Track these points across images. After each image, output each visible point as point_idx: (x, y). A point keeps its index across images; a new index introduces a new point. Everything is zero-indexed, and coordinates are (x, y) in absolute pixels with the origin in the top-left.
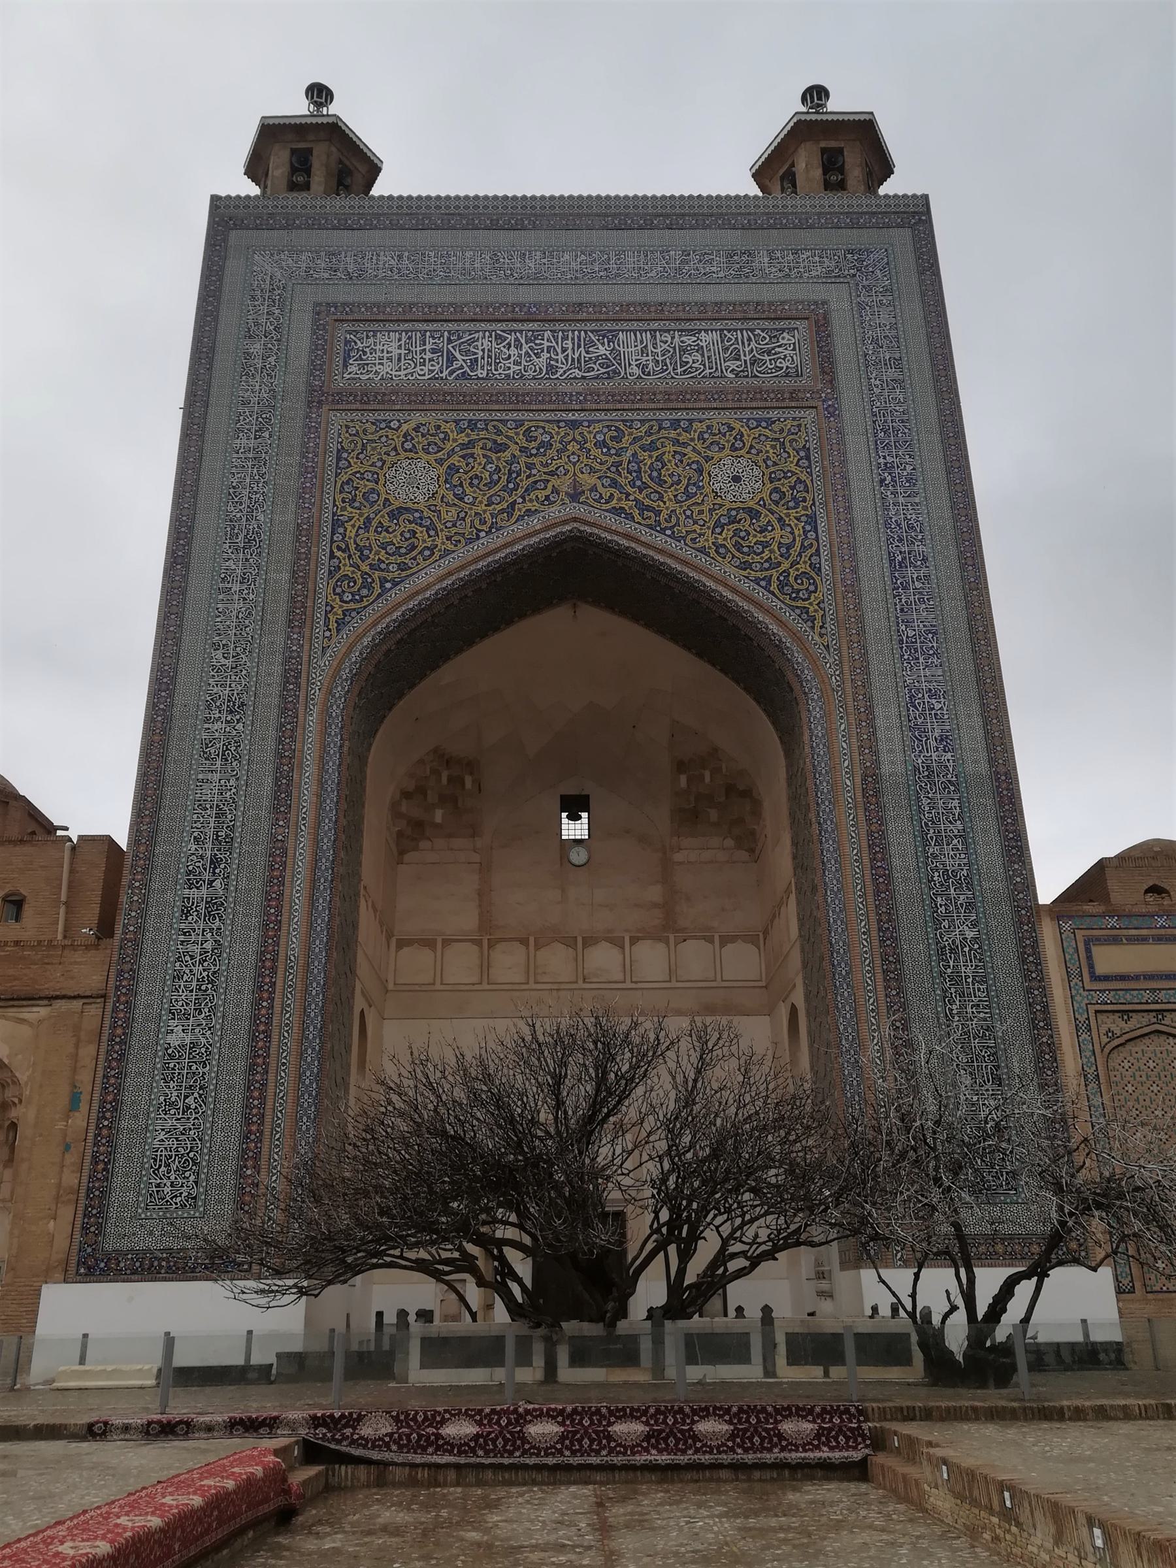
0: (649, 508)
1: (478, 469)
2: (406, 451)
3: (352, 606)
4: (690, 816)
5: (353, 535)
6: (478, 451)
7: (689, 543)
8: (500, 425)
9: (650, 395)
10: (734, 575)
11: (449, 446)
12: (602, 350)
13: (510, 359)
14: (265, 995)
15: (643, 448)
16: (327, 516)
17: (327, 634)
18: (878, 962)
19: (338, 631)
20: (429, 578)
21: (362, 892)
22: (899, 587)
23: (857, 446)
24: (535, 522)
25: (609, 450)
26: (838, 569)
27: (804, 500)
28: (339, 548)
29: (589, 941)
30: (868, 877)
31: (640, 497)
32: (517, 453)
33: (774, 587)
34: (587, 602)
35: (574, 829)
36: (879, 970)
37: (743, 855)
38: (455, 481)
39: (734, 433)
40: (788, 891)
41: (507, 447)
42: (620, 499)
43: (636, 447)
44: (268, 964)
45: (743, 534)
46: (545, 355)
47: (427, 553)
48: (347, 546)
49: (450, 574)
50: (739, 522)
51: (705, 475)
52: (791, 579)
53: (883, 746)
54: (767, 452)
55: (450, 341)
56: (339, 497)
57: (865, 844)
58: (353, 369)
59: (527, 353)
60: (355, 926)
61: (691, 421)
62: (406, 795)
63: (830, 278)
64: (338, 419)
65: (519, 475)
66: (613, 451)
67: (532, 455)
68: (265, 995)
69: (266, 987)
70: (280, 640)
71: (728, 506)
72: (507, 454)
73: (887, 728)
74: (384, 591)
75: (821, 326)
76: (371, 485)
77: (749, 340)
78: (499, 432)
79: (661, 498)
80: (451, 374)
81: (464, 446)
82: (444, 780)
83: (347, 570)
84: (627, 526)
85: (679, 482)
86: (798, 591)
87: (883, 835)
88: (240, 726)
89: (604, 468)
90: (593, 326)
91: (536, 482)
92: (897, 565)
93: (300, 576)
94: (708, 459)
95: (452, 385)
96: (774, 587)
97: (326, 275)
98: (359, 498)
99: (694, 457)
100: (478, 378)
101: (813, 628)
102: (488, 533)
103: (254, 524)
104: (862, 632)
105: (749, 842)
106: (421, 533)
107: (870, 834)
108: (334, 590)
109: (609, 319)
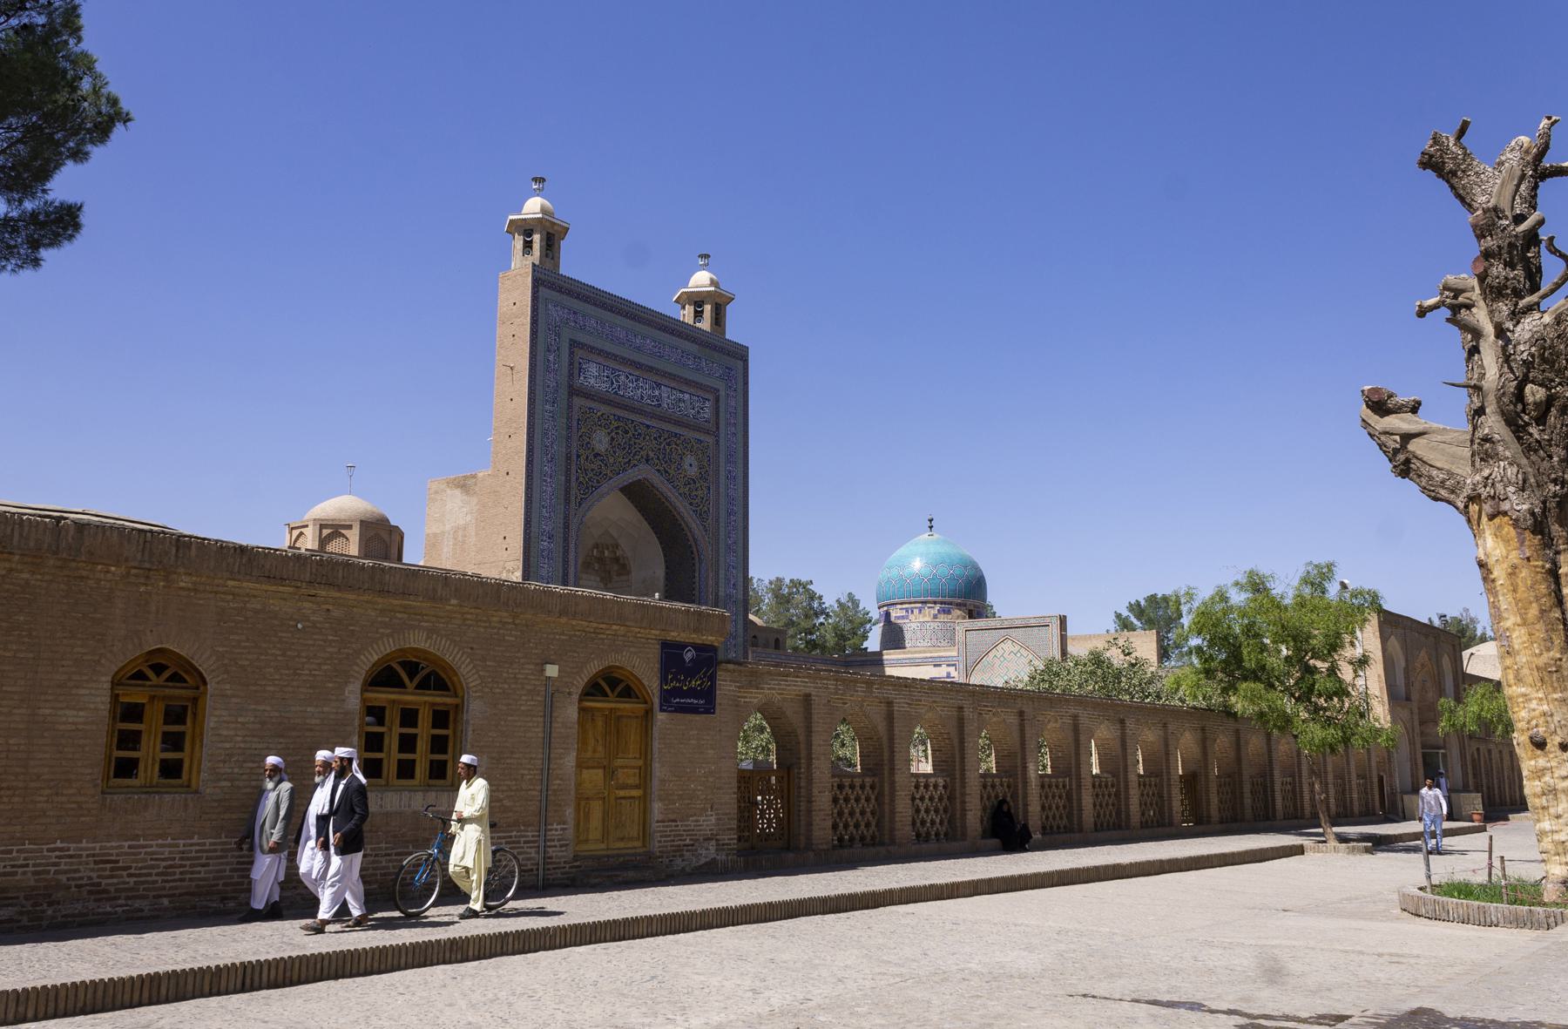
93: (568, 481)
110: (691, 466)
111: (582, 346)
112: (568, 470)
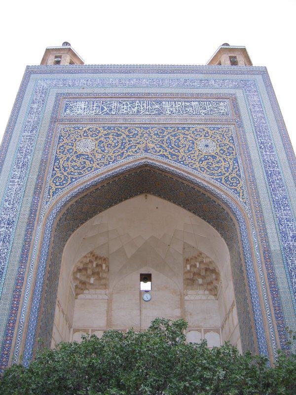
0: (174, 155)
1: (110, 142)
2: (84, 136)
3: (59, 187)
4: (190, 282)
5: (62, 163)
6: (111, 136)
7: (190, 166)
8: (119, 129)
10: (207, 177)
11: (100, 135)
12: (157, 107)
14: (9, 338)
15: (172, 136)
16: (54, 157)
17: (49, 197)
18: (276, 327)
19: (53, 195)
20: (89, 178)
21: (57, 303)
22: (271, 183)
24: (131, 159)
25: (159, 136)
26: (247, 176)
27: (233, 153)
28: (56, 168)
30: (269, 291)
31: (171, 151)
32: (125, 137)
33: (223, 181)
34: (151, 194)
35: (146, 286)
36: (276, 330)
37: (213, 297)
38: (102, 145)
39: (205, 131)
40: (233, 306)
41: (121, 135)
42: (163, 152)
43: (169, 135)
44: (11, 325)
45: (210, 164)
46: (136, 108)
47: (89, 169)
48: (60, 167)
49: (97, 176)
50: (208, 160)
51: (195, 144)
52: (230, 179)
53: (270, 239)
54: (218, 137)
55: (102, 103)
56: (58, 151)
57: (266, 278)
58: (68, 112)
59: (130, 107)
60: (53, 315)
61: (189, 128)
62: (79, 270)
63: (235, 87)
65: (125, 143)
66: (161, 136)
67: (130, 137)
68: (9, 338)
69: (9, 335)
70: (30, 199)
71: (204, 154)
72: (122, 137)
73: (272, 233)
74: (72, 182)
75: (234, 101)
76: (70, 147)
77: (209, 104)
78: (119, 130)
79: (179, 151)
80: (102, 113)
81: (105, 135)
82: (94, 265)
83: (59, 175)
84: (166, 161)
85: (185, 146)
86: (233, 183)
87: (274, 274)
88: (11, 230)
89: (157, 142)
90: (154, 99)
91: (132, 146)
92: (269, 175)
93: (41, 177)
94: (196, 139)
96: (223, 181)
97: (62, 86)
98: (66, 151)
99: (191, 139)
100: (112, 114)
101: (239, 196)
102: (113, 162)
103: (26, 159)
104: (258, 197)
105: (213, 289)
106: (88, 162)
107: (268, 274)
108: (53, 181)
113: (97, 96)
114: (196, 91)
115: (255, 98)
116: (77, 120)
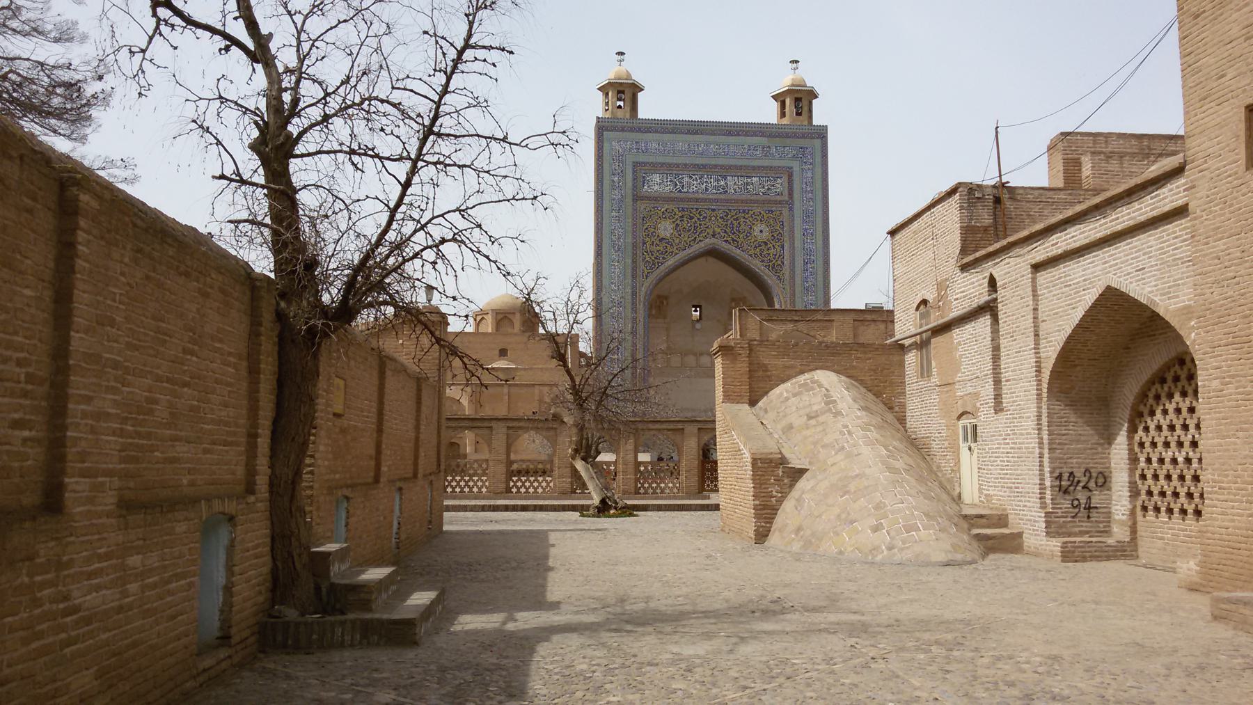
9: (736, 201)
13: (694, 185)
23: (798, 221)
24: (702, 244)
29: (701, 354)
64: (642, 206)
75: (790, 176)
92: (806, 263)
93: (634, 262)
95: (677, 195)
109: (724, 171)
110: (761, 231)
111: (645, 164)
112: (634, 254)
113: (670, 166)
114: (756, 163)
115: (810, 175)
116: (656, 199)
